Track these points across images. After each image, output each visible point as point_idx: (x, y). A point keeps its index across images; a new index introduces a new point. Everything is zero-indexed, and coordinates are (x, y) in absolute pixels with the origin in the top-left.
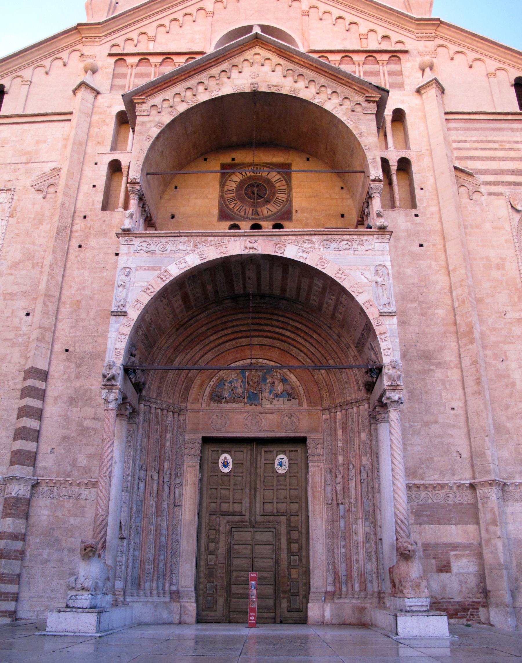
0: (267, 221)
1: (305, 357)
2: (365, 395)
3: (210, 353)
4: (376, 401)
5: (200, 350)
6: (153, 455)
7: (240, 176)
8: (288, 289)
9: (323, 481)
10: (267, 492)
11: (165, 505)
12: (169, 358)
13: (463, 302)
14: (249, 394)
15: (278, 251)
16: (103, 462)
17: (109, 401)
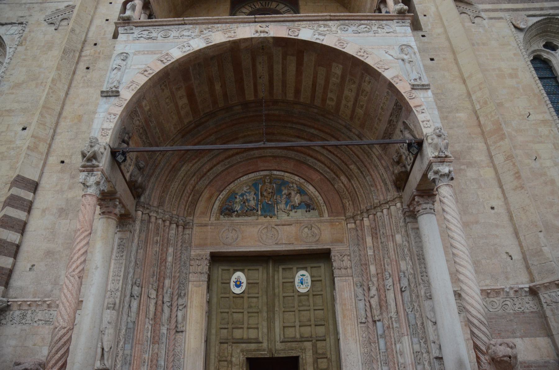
1: (323, 166)
2: (396, 194)
3: (220, 165)
4: (414, 190)
5: (208, 161)
6: (151, 270)
7: (250, 9)
8: (302, 90)
9: (353, 297)
10: (287, 315)
11: (164, 330)
12: (173, 167)
13: (486, 103)
14: (263, 206)
15: (291, 34)
16: (72, 258)
17: (88, 184)
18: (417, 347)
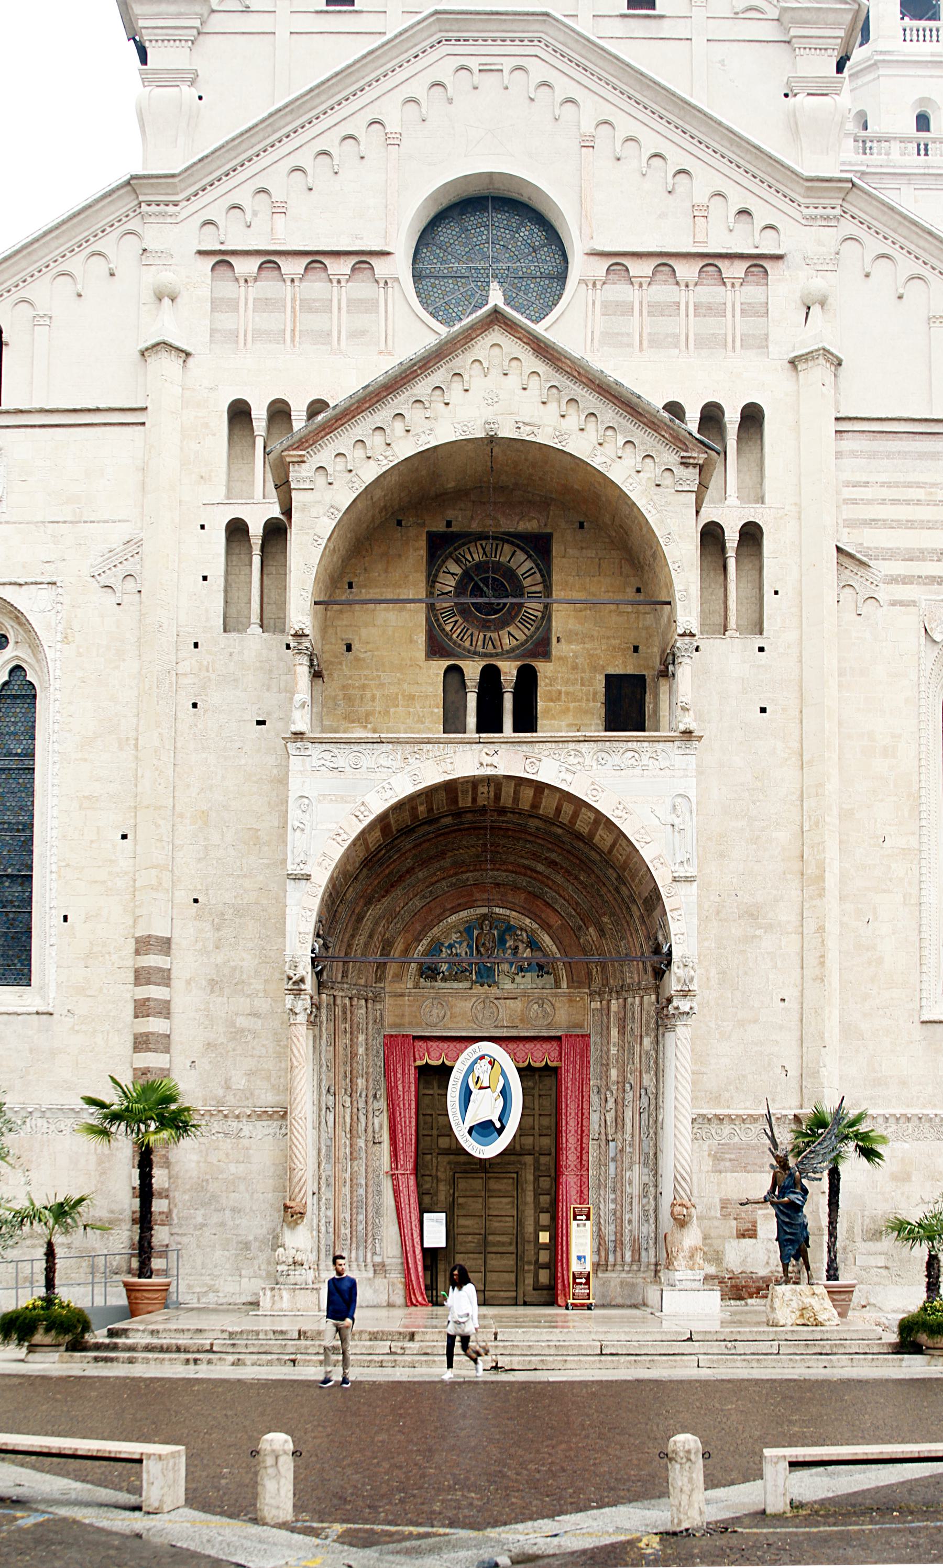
0: (509, 659)
14: (479, 968)
18: (645, 1179)
